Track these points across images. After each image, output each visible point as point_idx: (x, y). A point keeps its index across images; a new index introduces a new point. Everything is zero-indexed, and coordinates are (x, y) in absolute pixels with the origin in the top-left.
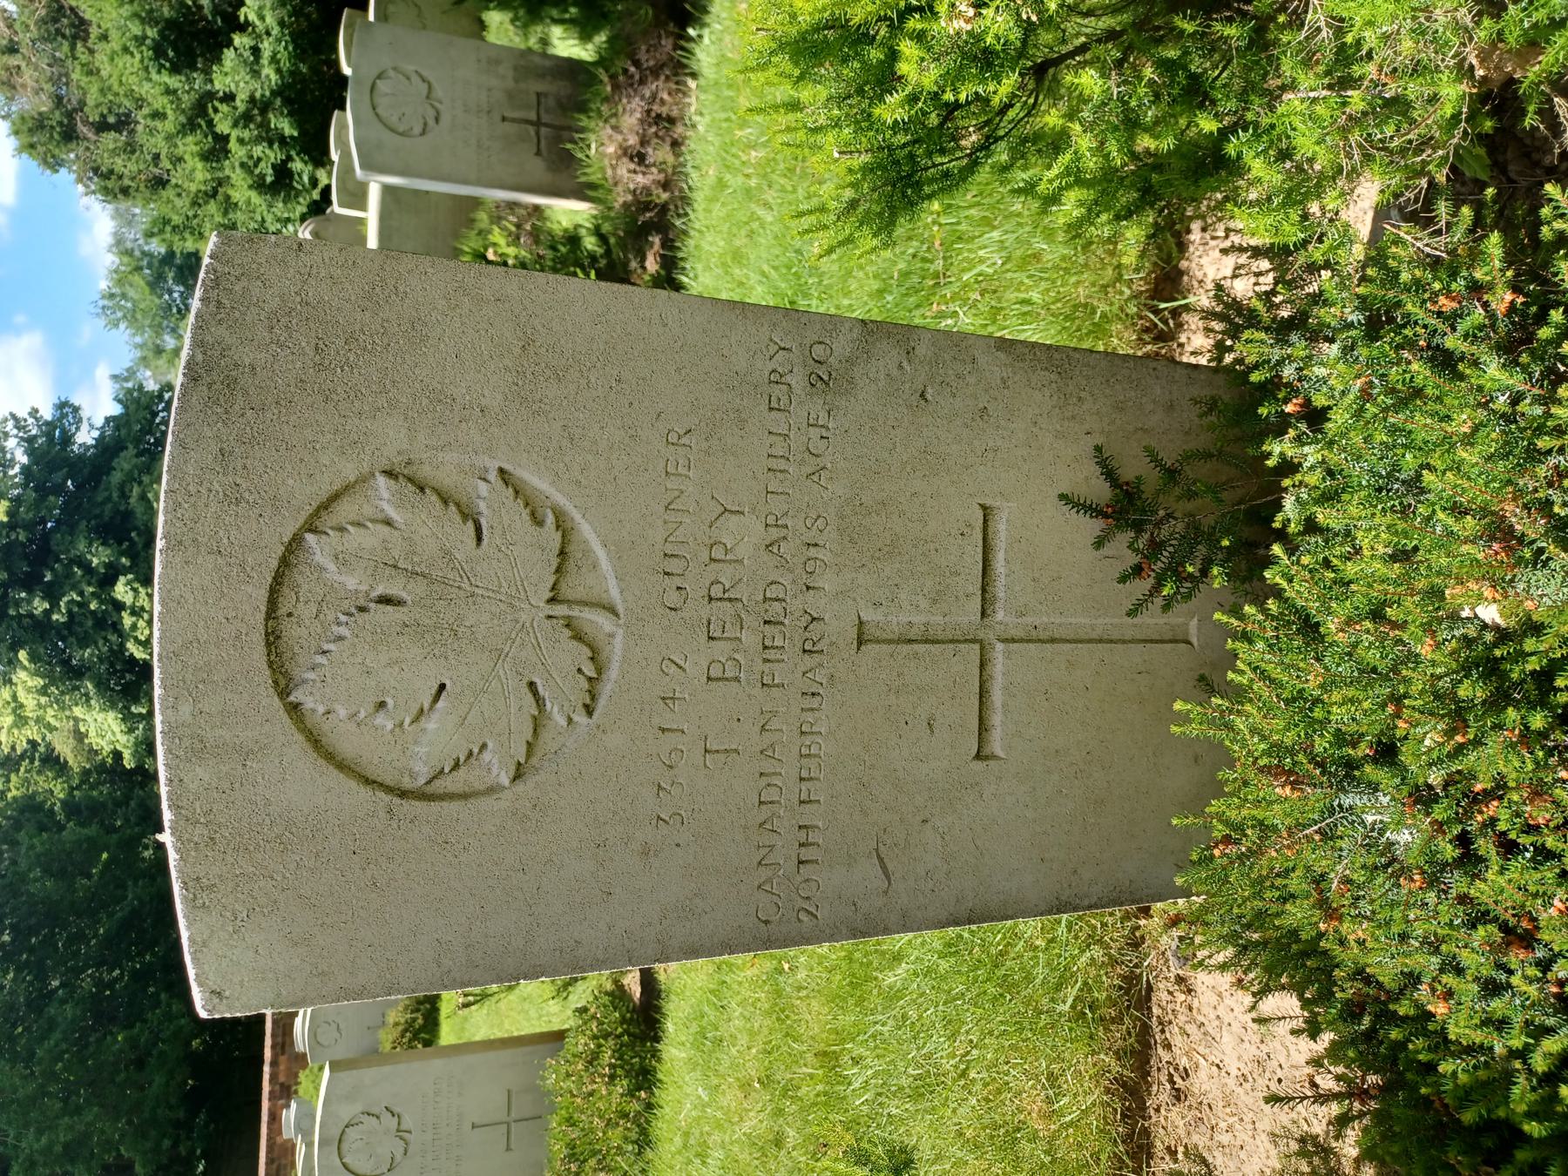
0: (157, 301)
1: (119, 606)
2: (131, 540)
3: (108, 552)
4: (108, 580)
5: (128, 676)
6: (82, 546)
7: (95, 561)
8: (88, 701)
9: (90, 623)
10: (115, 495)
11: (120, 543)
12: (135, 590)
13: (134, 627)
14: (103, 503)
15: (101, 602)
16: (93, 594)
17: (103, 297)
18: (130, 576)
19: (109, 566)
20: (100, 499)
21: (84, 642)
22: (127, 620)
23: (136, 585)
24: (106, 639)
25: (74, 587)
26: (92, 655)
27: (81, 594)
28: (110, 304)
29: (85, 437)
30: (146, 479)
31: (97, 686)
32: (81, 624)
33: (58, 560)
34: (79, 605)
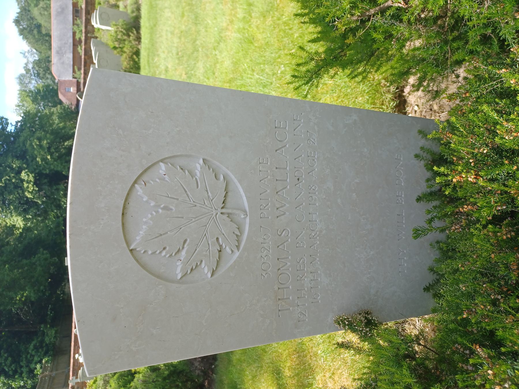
0: (34, 106)
1: (22, 181)
2: (27, 160)
3: (19, 162)
4: (19, 172)
5: (25, 206)
6: (10, 160)
7: (14, 166)
8: (11, 212)
9: (12, 186)
10: (21, 145)
11: (23, 161)
12: (28, 175)
13: (28, 187)
14: (17, 148)
15: (16, 180)
16: (13, 176)
17: (16, 106)
18: (26, 170)
19: (19, 167)
20: (16, 146)
21: (10, 193)
22: (26, 185)
23: (28, 173)
24: (18, 193)
25: (7, 175)
26: (13, 197)
27: (9, 177)
28: (18, 108)
29: (11, 128)
30: (32, 139)
31: (15, 208)
32: (9, 187)
33: (1, 166)
34: (9, 180)
